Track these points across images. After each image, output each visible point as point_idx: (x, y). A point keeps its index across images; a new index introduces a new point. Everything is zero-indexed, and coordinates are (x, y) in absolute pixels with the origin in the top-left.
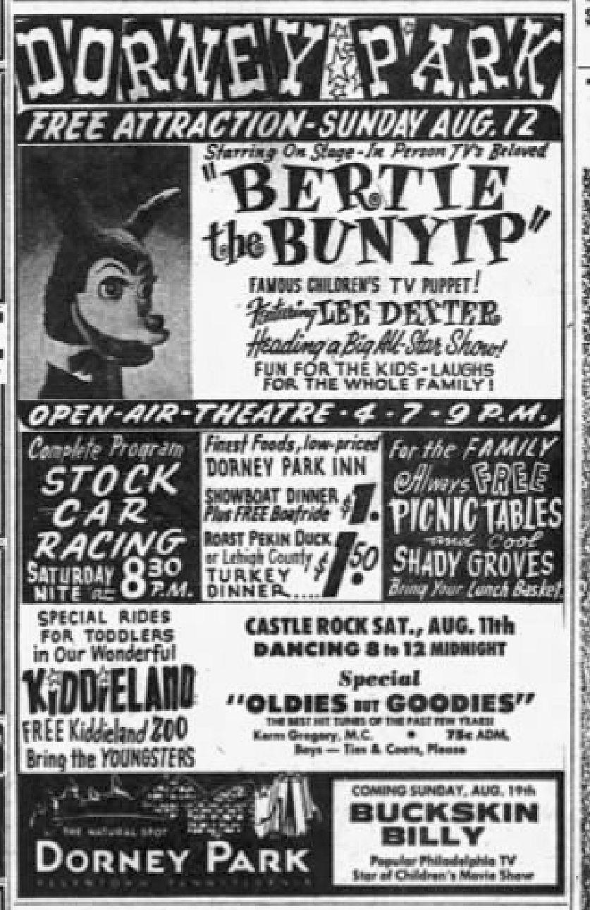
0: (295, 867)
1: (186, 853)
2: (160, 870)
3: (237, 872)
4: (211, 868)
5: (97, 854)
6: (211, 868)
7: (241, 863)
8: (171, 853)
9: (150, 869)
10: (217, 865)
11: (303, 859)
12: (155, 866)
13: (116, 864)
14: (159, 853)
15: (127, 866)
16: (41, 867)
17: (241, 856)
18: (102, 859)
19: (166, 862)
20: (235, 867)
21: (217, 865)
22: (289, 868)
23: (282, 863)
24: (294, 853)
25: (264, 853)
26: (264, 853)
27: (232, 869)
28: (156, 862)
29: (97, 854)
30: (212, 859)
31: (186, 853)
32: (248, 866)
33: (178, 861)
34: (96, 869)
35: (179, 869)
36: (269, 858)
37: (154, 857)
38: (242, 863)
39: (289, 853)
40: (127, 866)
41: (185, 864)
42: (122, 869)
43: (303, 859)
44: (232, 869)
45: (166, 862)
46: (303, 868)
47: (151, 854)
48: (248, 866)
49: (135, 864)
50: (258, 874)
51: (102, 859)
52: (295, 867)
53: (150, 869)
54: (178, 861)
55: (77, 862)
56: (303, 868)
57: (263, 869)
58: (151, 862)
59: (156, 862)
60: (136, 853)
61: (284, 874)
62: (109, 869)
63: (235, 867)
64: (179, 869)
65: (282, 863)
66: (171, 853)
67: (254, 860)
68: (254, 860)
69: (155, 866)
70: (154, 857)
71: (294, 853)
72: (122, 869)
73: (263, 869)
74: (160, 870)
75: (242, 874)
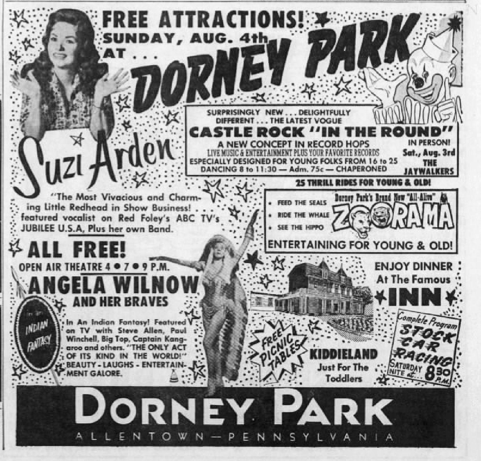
0: (375, 418)
1: (248, 403)
2: (220, 422)
3: (307, 423)
4: (278, 420)
5: (146, 402)
6: (278, 420)
7: (313, 414)
8: (232, 402)
9: (208, 421)
10: (285, 415)
11: (385, 410)
12: (212, 417)
13: (167, 415)
14: (219, 402)
15: (181, 417)
16: (81, 419)
17: (313, 405)
18: (153, 408)
19: (226, 412)
20: (305, 419)
21: (285, 415)
22: (369, 421)
23: (360, 415)
24: (374, 404)
25: (339, 403)
26: (339, 403)
27: (302, 422)
28: (215, 412)
29: (146, 402)
30: (280, 409)
31: (248, 403)
32: (322, 419)
33: (241, 411)
34: (145, 421)
35: (241, 421)
36: (346, 409)
37: (212, 407)
38: (313, 413)
39: (369, 402)
40: (181, 417)
41: (247, 415)
42: (175, 421)
43: (385, 410)
44: (302, 422)
45: (226, 412)
46: (385, 421)
47: (208, 402)
48: (322, 419)
49: (190, 415)
50: (332, 428)
51: (153, 408)
52: (375, 418)
53: (208, 421)
54: (241, 411)
55: (123, 411)
56: (385, 421)
57: (338, 421)
58: (208, 412)
59: (215, 412)
60: (192, 402)
61: (362, 428)
62: (160, 421)
63: (305, 419)
64: (241, 421)
65: (360, 415)
66: (232, 402)
67: (330, 413)
68: (330, 413)
69: (212, 417)
70: (212, 407)
71: (374, 404)
72: (175, 421)
73: (338, 421)
74: (220, 422)
75: (313, 427)
